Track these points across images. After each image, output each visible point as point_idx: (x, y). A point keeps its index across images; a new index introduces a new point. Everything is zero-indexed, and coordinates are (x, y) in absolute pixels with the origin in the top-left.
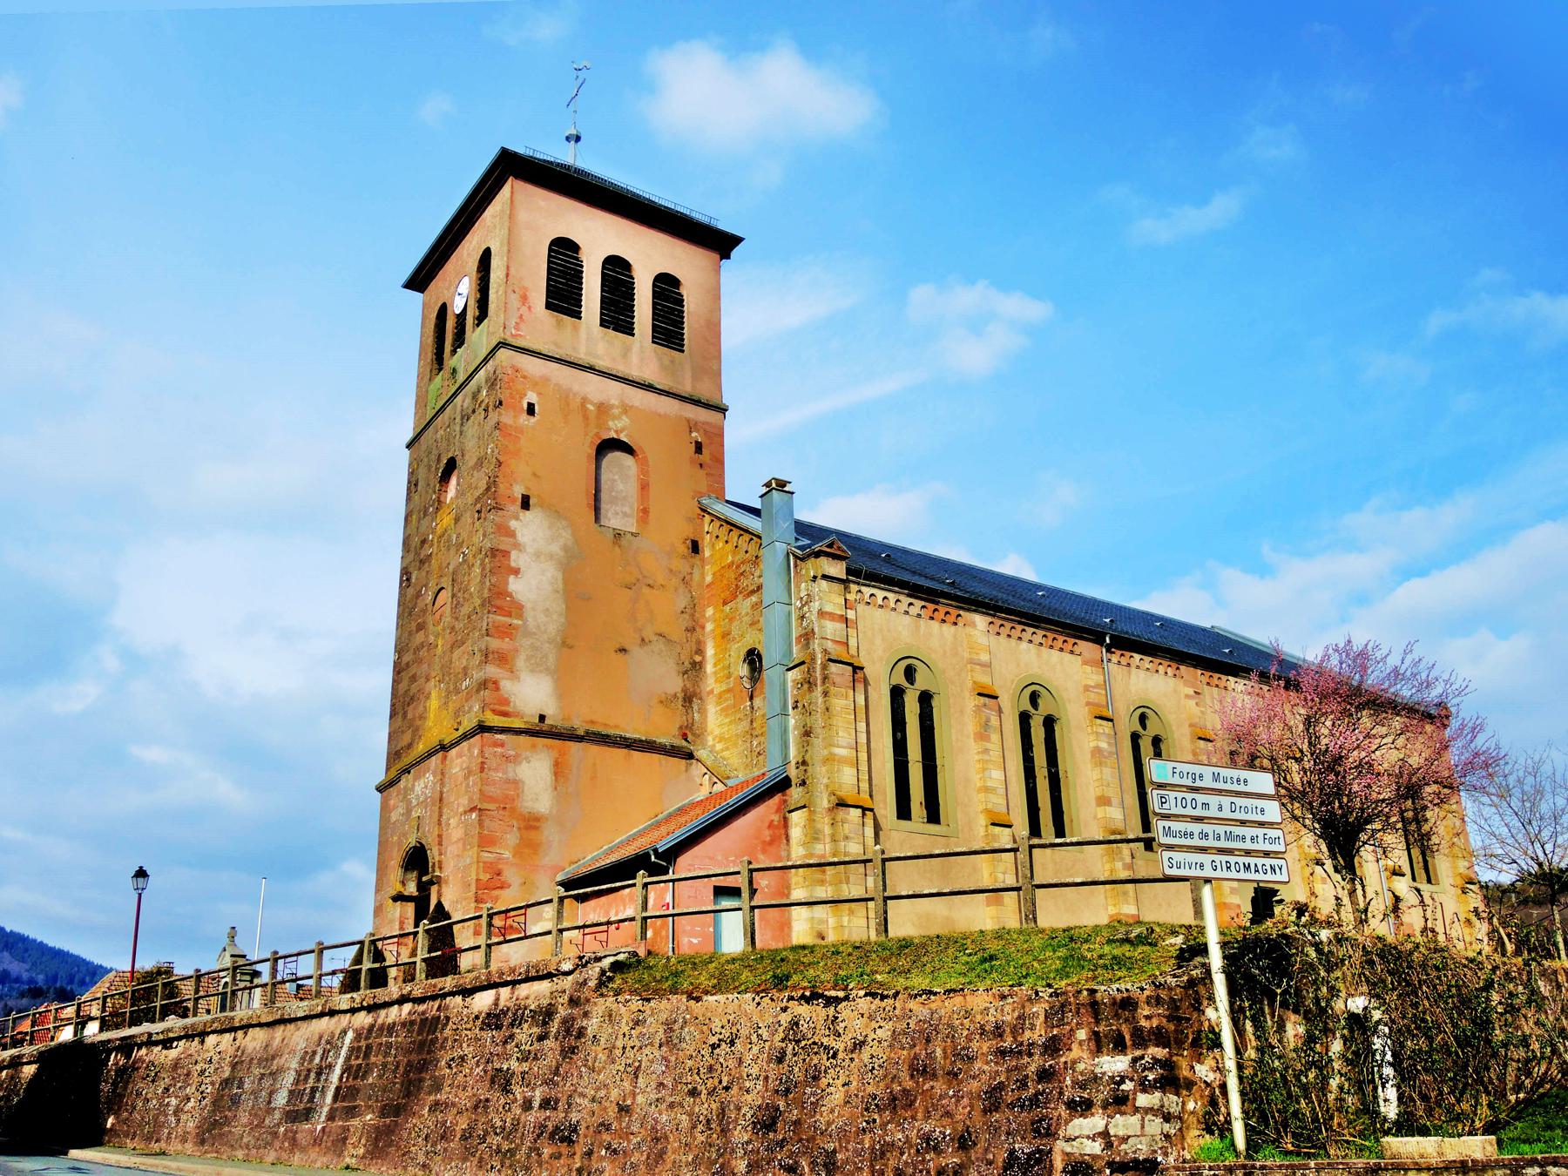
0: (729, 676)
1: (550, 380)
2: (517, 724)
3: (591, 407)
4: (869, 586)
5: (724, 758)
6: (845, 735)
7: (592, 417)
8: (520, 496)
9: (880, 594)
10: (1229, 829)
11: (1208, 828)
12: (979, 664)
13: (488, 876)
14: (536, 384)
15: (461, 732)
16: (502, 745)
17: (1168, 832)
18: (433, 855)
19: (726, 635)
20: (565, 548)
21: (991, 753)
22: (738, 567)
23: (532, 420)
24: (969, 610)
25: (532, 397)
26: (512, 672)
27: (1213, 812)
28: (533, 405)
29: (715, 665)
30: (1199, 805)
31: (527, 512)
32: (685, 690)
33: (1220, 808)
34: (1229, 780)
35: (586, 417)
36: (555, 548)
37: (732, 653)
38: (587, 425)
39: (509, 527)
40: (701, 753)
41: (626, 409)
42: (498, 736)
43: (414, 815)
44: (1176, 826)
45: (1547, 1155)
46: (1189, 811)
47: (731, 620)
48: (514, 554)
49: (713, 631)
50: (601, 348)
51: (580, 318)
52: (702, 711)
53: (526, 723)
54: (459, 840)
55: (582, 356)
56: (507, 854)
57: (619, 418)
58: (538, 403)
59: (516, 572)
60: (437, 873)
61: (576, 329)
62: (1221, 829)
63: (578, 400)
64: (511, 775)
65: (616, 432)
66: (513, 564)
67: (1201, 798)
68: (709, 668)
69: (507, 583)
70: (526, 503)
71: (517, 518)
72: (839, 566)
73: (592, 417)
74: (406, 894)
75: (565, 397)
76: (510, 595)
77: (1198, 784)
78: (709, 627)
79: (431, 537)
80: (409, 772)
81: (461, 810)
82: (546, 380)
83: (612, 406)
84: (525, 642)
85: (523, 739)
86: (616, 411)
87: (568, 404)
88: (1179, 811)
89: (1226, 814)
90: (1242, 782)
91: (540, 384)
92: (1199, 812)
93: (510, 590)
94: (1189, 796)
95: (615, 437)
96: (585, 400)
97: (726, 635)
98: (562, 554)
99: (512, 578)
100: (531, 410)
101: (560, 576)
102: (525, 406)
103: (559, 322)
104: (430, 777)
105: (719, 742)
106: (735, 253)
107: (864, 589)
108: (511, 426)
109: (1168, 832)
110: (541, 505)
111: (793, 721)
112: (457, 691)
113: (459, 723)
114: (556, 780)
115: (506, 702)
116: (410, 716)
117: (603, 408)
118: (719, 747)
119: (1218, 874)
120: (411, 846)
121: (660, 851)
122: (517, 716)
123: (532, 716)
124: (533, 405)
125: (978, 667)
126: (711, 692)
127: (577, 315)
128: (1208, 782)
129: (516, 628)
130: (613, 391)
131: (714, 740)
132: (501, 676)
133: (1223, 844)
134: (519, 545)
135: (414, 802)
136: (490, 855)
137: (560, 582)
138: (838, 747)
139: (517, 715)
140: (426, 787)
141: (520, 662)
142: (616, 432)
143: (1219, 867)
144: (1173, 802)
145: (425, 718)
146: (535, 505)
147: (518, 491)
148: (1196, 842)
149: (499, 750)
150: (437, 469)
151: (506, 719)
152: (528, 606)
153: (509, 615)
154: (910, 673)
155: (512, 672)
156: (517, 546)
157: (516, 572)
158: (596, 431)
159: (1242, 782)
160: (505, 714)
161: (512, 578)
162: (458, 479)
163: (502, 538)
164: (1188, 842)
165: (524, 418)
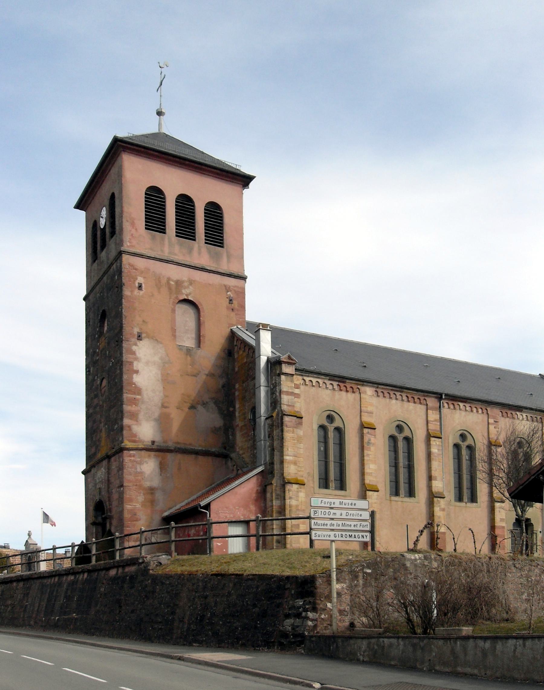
0: (245, 418)
1: (149, 270)
2: (141, 446)
3: (172, 283)
4: (308, 376)
5: (243, 458)
6: (292, 450)
7: (173, 288)
8: (137, 333)
9: (314, 380)
10: (344, 522)
11: (333, 522)
12: (367, 412)
13: (130, 516)
14: (142, 272)
15: (114, 450)
16: (134, 456)
17: (316, 524)
18: (107, 505)
19: (244, 398)
20: (161, 358)
21: (370, 456)
22: (249, 365)
23: (141, 293)
24: (363, 385)
25: (140, 280)
26: (137, 421)
27: (338, 516)
28: (141, 284)
29: (239, 413)
30: (332, 514)
31: (141, 342)
32: (225, 425)
33: (341, 515)
34: (347, 504)
35: (170, 289)
36: (156, 359)
37: (246, 407)
38: (171, 293)
39: (132, 350)
40: (233, 455)
41: (191, 282)
42: (131, 452)
43: (98, 487)
44: (320, 522)
45: (454, 628)
46: (327, 516)
47: (246, 391)
48: (135, 364)
49: (238, 395)
50: (177, 249)
51: (165, 233)
52: (234, 435)
53: (144, 445)
54: (117, 499)
55: (166, 255)
56: (138, 506)
57: (187, 287)
58: (144, 283)
59: (137, 372)
60: (109, 514)
61: (163, 240)
62: (340, 523)
63: (166, 279)
64: (139, 470)
65: (187, 295)
66: (135, 368)
67: (332, 511)
68: (237, 414)
69: (132, 378)
70: (139, 337)
71: (136, 345)
72: (291, 368)
73: (173, 288)
74: (97, 522)
75: (158, 281)
76: (135, 384)
77: (332, 506)
78: (237, 393)
79: (97, 350)
80: (95, 467)
81: (117, 486)
82: (147, 270)
83: (183, 282)
84: (143, 407)
85: (143, 452)
86: (186, 284)
87: (160, 282)
88: (323, 516)
89: (344, 516)
90: (353, 505)
91: (145, 272)
92: (331, 516)
93: (134, 382)
94: (327, 511)
95: (186, 298)
96: (169, 279)
97: (244, 398)
98: (160, 361)
99: (135, 376)
100: (140, 287)
101: (159, 373)
102: (137, 285)
103: (153, 238)
104: (103, 470)
105: (241, 450)
106: (252, 184)
107: (305, 378)
108: (130, 296)
109: (316, 524)
110: (148, 337)
111: (268, 443)
112: (113, 430)
113: (115, 446)
114: (161, 471)
115: (135, 435)
116: (94, 439)
117: (179, 284)
118: (241, 452)
119: (337, 538)
120: (97, 501)
121: (202, 506)
122: (140, 442)
123: (148, 442)
124: (141, 284)
125: (366, 414)
126: (238, 426)
127: (163, 231)
128: (337, 505)
129: (138, 400)
130: (184, 274)
131: (239, 449)
132: (132, 423)
133: (341, 528)
134: (138, 358)
135: (98, 481)
136: (130, 506)
137: (160, 376)
138: (288, 456)
139: (140, 441)
140: (102, 474)
141: (141, 416)
142: (187, 295)
143: (337, 536)
144: (320, 513)
145: (101, 441)
146: (145, 337)
147: (136, 330)
148: (328, 527)
149: (132, 458)
150: (98, 315)
151: (134, 444)
152: (144, 389)
153: (134, 393)
154: (330, 418)
155: (137, 421)
156: (137, 359)
157: (137, 372)
158: (175, 295)
159: (353, 505)
160: (134, 441)
161: (135, 376)
162: (107, 321)
163: (129, 356)
164: (325, 527)
165: (136, 292)
